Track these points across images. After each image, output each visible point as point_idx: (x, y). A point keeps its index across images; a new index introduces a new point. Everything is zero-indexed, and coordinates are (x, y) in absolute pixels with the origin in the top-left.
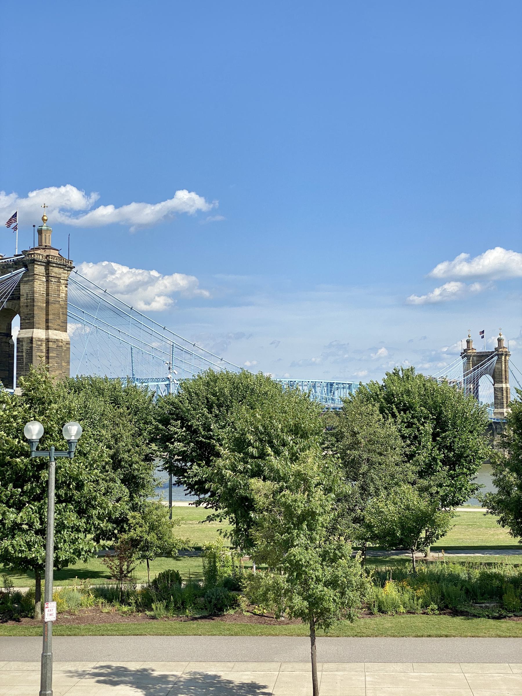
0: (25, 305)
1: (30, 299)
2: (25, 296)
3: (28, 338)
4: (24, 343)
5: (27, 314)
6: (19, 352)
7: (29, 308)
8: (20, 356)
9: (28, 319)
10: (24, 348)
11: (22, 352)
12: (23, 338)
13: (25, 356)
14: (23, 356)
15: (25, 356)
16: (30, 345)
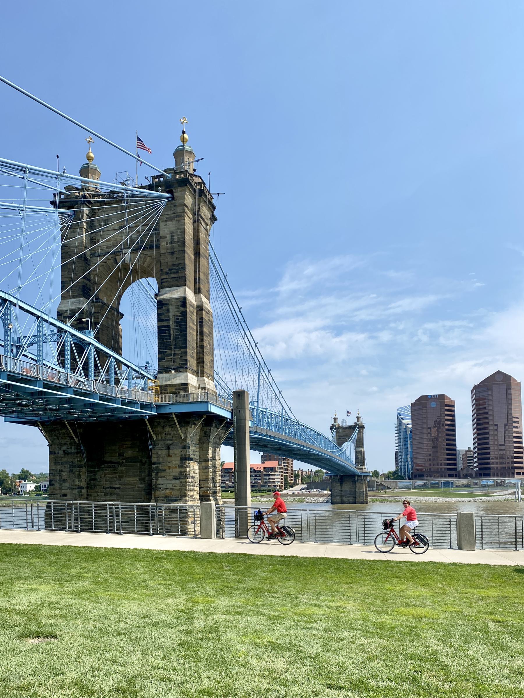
0: (169, 251)
1: (178, 242)
2: (169, 237)
3: (177, 299)
4: (170, 307)
5: (173, 265)
6: (163, 320)
7: (176, 255)
8: (164, 326)
9: (174, 273)
10: (171, 314)
11: (168, 320)
12: (169, 300)
13: (172, 327)
14: (169, 326)
15: (172, 327)
16: (182, 309)
